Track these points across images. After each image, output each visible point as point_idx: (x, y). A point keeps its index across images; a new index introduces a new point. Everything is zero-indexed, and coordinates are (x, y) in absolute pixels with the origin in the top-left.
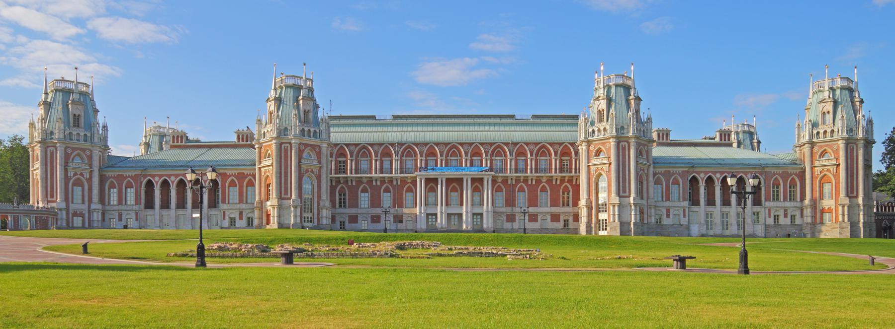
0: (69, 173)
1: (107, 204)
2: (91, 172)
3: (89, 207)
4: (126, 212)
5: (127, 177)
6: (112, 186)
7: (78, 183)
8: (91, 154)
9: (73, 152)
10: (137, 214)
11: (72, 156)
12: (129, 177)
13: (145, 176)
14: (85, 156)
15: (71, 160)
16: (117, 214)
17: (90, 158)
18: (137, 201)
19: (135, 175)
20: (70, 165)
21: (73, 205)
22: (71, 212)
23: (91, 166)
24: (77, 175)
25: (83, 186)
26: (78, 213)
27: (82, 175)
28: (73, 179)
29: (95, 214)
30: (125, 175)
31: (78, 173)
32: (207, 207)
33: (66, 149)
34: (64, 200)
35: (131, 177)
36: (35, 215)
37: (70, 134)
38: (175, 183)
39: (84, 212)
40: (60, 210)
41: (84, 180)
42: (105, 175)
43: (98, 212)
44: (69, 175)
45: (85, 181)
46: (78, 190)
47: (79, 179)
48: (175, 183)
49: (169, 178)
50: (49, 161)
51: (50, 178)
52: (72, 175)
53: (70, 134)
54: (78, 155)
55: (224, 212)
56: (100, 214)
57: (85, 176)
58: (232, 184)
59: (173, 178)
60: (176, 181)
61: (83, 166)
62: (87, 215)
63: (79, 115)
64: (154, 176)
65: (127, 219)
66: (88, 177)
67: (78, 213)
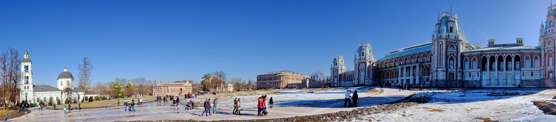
0: (448, 53)
1: (464, 69)
6: (466, 60)
7: (452, 59)
9: (450, 43)
11: (450, 45)
15: (449, 47)
18: (478, 68)
21: (450, 69)
24: (452, 55)
25: (454, 60)
27: (453, 55)
31: (452, 54)
35: (476, 56)
42: (463, 55)
46: (451, 62)
48: (497, 58)
49: (487, 55)
54: (452, 45)
55: (523, 72)
56: (461, 73)
57: (455, 55)
58: (527, 58)
59: (496, 55)
60: (498, 56)
61: (454, 51)
64: (486, 54)
65: (473, 76)
66: (456, 55)
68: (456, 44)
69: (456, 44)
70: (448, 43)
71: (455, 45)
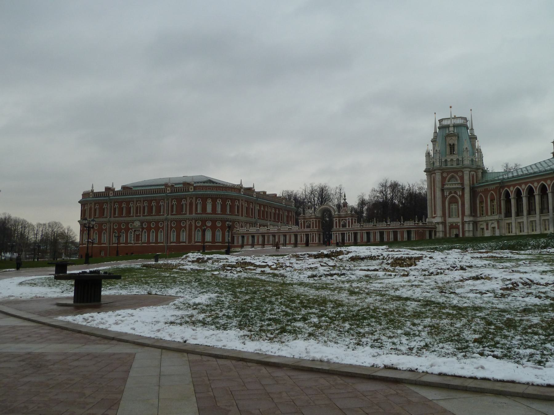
1: (478, 215)
2: (463, 189)
3: (463, 219)
4: (491, 222)
5: (490, 190)
7: (453, 200)
8: (463, 175)
10: (498, 222)
11: (447, 179)
12: (492, 190)
13: (503, 187)
14: (457, 177)
16: (485, 224)
17: (462, 178)
19: (496, 187)
20: (446, 186)
22: (448, 225)
23: (462, 184)
24: (452, 193)
25: (457, 202)
26: (454, 225)
27: (455, 193)
28: (449, 197)
29: (466, 225)
30: (489, 189)
31: (453, 192)
32: (552, 211)
33: (442, 174)
34: (442, 215)
36: (414, 230)
37: (446, 161)
38: (525, 190)
39: (459, 224)
40: (438, 223)
41: (458, 197)
43: (469, 223)
44: (445, 195)
45: (458, 197)
47: (453, 197)
50: (432, 185)
51: (434, 199)
52: (448, 194)
53: (446, 161)
54: (453, 177)
57: (458, 194)
61: (457, 186)
62: (461, 226)
63: (454, 145)
66: (461, 194)
67: (454, 225)
68: (460, 174)
69: (460, 174)
70: (445, 175)
71: (458, 176)
